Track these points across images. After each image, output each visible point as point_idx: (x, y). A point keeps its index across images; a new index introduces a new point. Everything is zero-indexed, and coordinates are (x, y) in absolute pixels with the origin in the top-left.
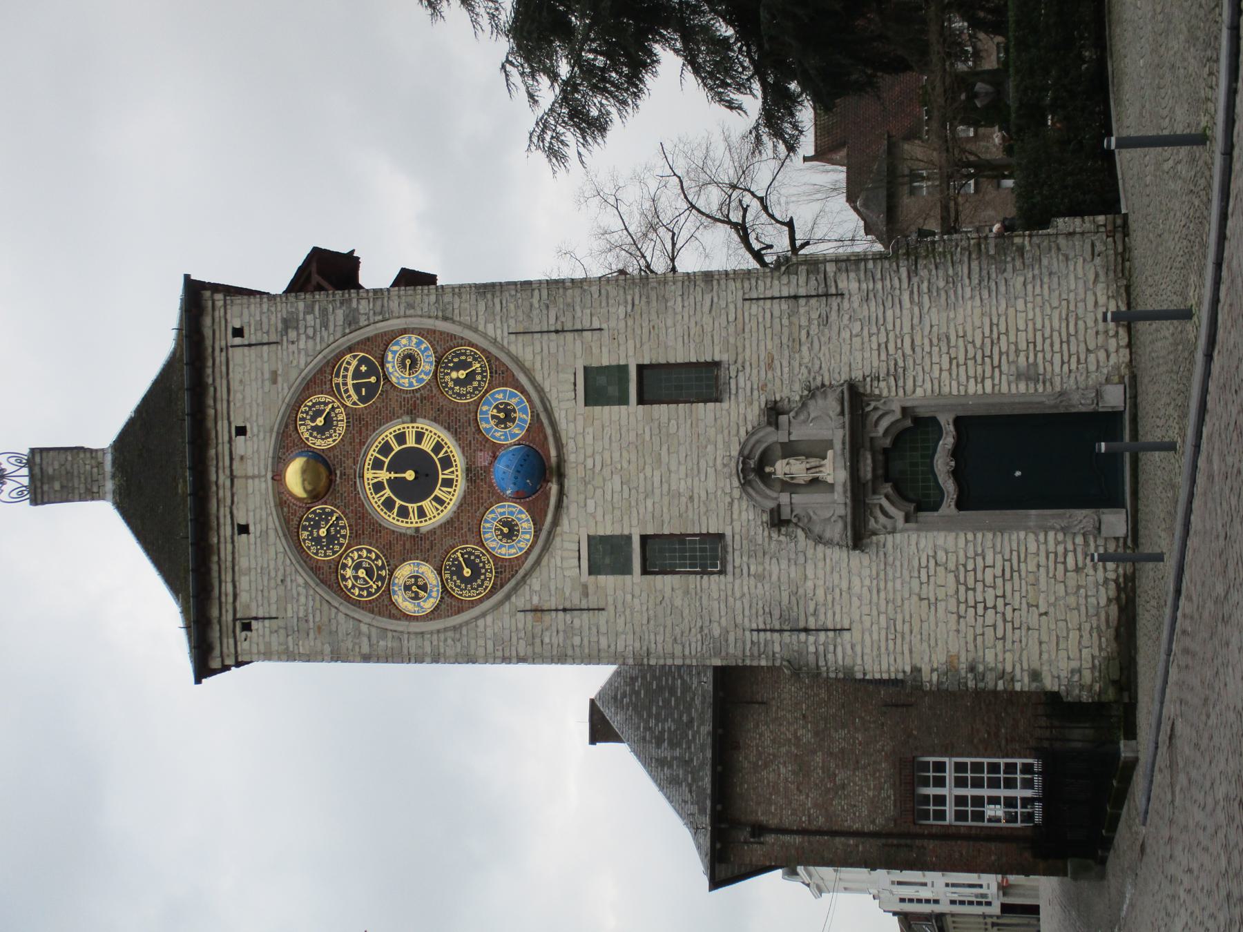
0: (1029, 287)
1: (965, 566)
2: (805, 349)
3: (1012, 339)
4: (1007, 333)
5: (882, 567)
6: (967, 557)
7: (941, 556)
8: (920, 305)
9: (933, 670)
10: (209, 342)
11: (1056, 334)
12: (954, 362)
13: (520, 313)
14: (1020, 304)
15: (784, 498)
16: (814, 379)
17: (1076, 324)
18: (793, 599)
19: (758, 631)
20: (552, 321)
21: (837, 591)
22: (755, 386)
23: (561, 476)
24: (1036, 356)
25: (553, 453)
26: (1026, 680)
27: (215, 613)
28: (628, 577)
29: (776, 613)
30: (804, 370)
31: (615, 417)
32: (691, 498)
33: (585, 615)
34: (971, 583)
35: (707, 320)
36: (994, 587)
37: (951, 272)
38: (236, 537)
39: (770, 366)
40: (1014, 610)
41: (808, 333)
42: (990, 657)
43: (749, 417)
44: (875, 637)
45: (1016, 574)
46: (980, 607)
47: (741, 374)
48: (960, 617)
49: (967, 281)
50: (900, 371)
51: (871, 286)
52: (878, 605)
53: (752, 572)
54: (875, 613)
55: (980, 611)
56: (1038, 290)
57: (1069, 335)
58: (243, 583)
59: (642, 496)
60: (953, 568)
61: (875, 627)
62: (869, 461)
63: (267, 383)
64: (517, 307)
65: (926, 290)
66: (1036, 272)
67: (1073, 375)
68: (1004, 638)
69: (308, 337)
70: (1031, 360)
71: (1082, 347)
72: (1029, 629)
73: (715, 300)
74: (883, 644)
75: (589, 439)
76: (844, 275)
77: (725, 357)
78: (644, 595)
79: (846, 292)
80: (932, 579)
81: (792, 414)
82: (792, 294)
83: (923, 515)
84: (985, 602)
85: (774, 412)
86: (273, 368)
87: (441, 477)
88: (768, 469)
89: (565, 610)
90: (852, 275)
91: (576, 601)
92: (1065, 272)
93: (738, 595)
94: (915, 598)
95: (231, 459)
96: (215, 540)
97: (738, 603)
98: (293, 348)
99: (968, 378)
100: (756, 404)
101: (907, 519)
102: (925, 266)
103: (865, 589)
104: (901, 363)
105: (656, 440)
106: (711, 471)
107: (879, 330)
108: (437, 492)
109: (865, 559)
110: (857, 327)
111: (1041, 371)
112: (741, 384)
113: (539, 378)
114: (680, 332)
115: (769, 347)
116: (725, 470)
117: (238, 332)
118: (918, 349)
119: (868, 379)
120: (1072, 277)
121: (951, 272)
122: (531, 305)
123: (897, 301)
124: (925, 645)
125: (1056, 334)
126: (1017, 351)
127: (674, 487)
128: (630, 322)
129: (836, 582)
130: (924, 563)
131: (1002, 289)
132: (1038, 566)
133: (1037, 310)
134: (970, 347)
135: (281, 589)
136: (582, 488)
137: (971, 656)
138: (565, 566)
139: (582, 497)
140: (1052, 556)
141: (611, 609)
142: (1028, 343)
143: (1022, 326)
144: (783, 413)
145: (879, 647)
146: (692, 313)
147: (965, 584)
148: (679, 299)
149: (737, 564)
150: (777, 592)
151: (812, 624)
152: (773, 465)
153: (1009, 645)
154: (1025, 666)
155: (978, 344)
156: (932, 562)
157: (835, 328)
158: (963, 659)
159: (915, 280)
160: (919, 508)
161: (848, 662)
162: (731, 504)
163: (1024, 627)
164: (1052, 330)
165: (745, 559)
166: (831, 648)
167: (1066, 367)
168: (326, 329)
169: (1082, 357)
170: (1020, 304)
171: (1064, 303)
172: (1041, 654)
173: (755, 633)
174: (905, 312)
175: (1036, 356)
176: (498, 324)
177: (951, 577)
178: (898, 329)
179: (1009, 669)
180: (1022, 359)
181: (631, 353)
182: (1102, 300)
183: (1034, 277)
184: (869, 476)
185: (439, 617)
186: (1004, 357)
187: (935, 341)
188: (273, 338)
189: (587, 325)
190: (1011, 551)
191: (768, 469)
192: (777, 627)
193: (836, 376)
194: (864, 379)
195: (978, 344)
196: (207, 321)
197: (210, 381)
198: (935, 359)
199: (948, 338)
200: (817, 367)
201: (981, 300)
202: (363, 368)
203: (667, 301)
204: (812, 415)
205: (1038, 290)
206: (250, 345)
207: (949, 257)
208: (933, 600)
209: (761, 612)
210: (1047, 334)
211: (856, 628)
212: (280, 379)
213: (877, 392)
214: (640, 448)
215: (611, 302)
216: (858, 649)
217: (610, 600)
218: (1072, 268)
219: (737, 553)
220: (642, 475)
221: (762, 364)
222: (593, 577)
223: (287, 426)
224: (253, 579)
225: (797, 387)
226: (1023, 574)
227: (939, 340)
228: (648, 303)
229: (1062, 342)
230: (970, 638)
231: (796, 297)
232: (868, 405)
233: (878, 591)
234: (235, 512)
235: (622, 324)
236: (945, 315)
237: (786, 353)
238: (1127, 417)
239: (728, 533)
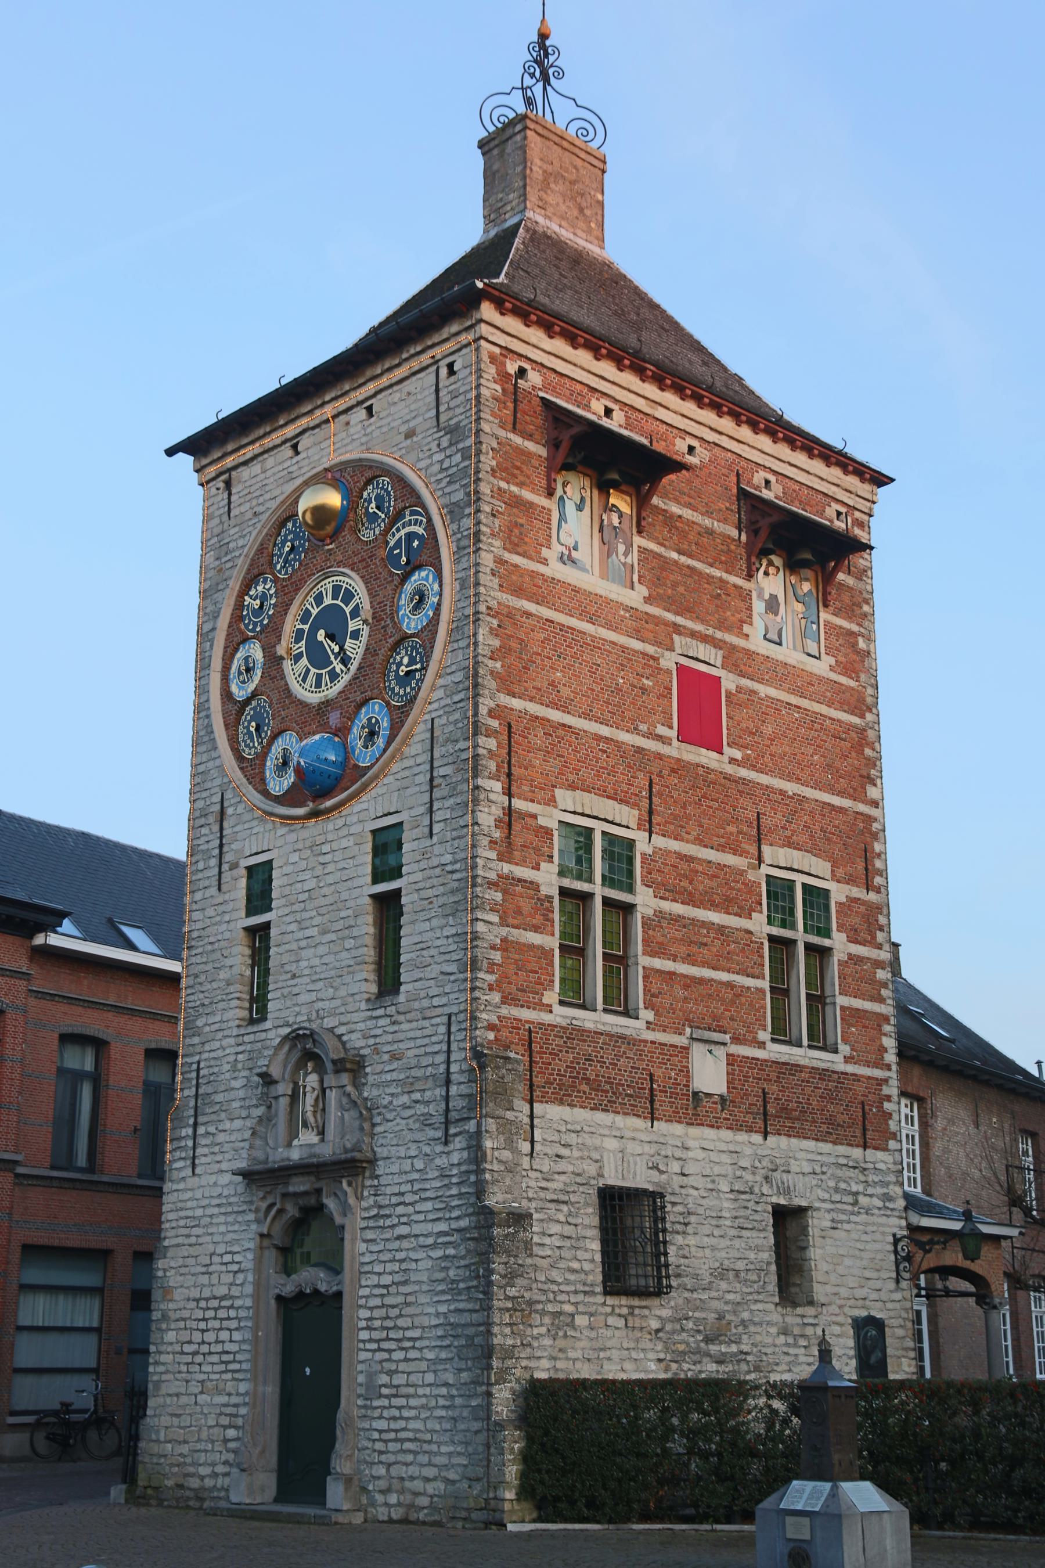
0: (444, 1391)
1: (232, 1307)
2: (405, 1099)
3: (402, 1367)
4: (406, 1360)
5: (236, 1209)
6: (238, 1308)
7: (240, 1277)
8: (434, 1246)
9: (165, 1270)
10: (436, 339)
11: (402, 1424)
12: (385, 1291)
13: (451, 728)
14: (430, 1378)
15: (284, 1088)
16: (379, 1114)
17: (410, 1451)
18: (217, 1107)
19: (198, 1070)
20: (442, 771)
21: (219, 1158)
22: (378, 1040)
23: (315, 814)
24: (387, 1397)
25: (329, 803)
26: (155, 1378)
27: (230, 447)
28: (243, 914)
29: (209, 1089)
30: (388, 1099)
31: (360, 871)
32: (294, 976)
33: (216, 871)
34: (222, 1314)
35: (434, 971)
36: (217, 1342)
37: (462, 1285)
38: (288, 444)
39: (395, 1057)
40: (200, 1365)
41: (417, 1102)
42: (171, 1336)
43: (354, 1036)
44: (189, 1204)
45: (223, 1367)
46: (202, 1325)
47: (388, 1020)
48: (197, 1300)
49: (452, 1307)
50: (381, 1223)
51: (454, 1180)
52: (209, 1205)
53: (240, 1057)
54: (206, 1202)
55: (202, 1325)
56: (442, 1402)
57: (402, 1441)
58: (256, 468)
59: (298, 917)
60: (232, 1293)
61: (194, 1204)
62: (302, 1188)
63: (403, 429)
64: (456, 722)
65: (447, 1252)
66: (458, 1401)
67: (370, 1445)
68: (183, 1353)
69: (442, 462)
70: (385, 1391)
71: (392, 1458)
72: (187, 1381)
73: (452, 978)
74: (182, 1214)
75: (344, 843)
76: (464, 1145)
77: (402, 998)
78: (227, 935)
79: (451, 1147)
80: (224, 1268)
81: (349, 1089)
82: (453, 1077)
83: (271, 1256)
84: (207, 1330)
85: (353, 1066)
86: (418, 431)
87: (323, 671)
88: (310, 1065)
89: (221, 846)
90: (465, 1154)
91: (228, 857)
92: (456, 1438)
93: (225, 1043)
94: (211, 1248)
95: (346, 411)
96: (281, 422)
97: (217, 1044)
98: (434, 446)
99: (371, 1309)
100: (362, 1043)
101: (262, 1235)
102: (468, 1251)
103: (219, 1190)
104: (388, 1222)
105: (340, 925)
106: (313, 996)
107: (415, 1193)
108: (313, 670)
109: (241, 1189)
110: (419, 1164)
111: (375, 1403)
112: (382, 1022)
113: (395, 767)
114: (427, 936)
115: (410, 1053)
116: (314, 1014)
117: (451, 372)
118: (396, 1245)
119: (376, 1182)
120: (451, 1449)
121: (462, 1285)
122: (457, 741)
123: (440, 1215)
124: (181, 1262)
125: (402, 1424)
126: (391, 1373)
127: (304, 954)
128: (438, 871)
129: (227, 1156)
130: (237, 1258)
131: (443, 1355)
132: (229, 1394)
133: (424, 1400)
134: (396, 1311)
135: (249, 515)
136: (308, 844)
137: (171, 1314)
138: (255, 838)
139: (300, 846)
140: (233, 1410)
141: (220, 900)
142: (397, 1387)
143: (413, 1378)
144: (355, 1078)
145: (182, 1209)
146: (442, 950)
147: (220, 1307)
148: (453, 931)
149: (246, 1039)
150: (223, 1088)
151: (201, 1130)
152: (314, 1071)
153: (179, 1358)
154: (164, 1377)
155: (400, 1322)
156: (235, 1267)
157: (419, 1136)
158: (171, 1306)
159: (455, 1237)
160: (284, 1251)
161: (175, 1175)
162: (288, 1025)
163: (189, 1377)
164: (407, 1419)
165: (249, 1047)
166: (183, 1155)
167: (376, 1435)
168: (449, 483)
169: (383, 1458)
170: (430, 1378)
171: (428, 1437)
172: (170, 1395)
173: (195, 1066)
174: (430, 1225)
175: (387, 1397)
176: (443, 703)
177: (223, 1291)
178: (415, 1217)
179: (163, 1358)
180: (384, 1379)
181: (412, 878)
182: (430, 1489)
183: (453, 1397)
184: (291, 1189)
185: (223, 703)
186: (386, 1355)
187: (404, 1266)
188: (443, 418)
189: (437, 817)
190: (240, 1362)
191: (310, 1065)
192: (201, 1091)
193: (381, 1141)
194: (377, 1177)
195: (400, 1322)
196: (454, 328)
197: (405, 356)
198: (389, 1267)
199: (405, 1283)
200: (389, 1116)
201: (436, 1326)
202: (416, 544)
203: (453, 915)
204: (346, 1115)
205: (442, 1402)
206: (437, 391)
207: (475, 1283)
208: (211, 1269)
209: (211, 1071)
210: (406, 1413)
211: (196, 1179)
212: (409, 441)
213: (366, 1193)
214: (334, 907)
215: (456, 843)
216: (181, 1186)
217: (227, 897)
218: (459, 1449)
219: (251, 1037)
220: (314, 913)
221: (395, 1047)
222: (244, 872)
223: (370, 467)
224: (258, 479)
225: (375, 1092)
226: (224, 1376)
227: (405, 1271)
228: (452, 892)
229: (396, 1431)
230: (186, 1314)
231: (448, 1082)
232: (350, 1184)
233: (218, 1205)
234: (307, 435)
235: (435, 861)
236: (425, 1279)
237: (402, 1076)
238: (311, 1511)
239: (268, 1025)
